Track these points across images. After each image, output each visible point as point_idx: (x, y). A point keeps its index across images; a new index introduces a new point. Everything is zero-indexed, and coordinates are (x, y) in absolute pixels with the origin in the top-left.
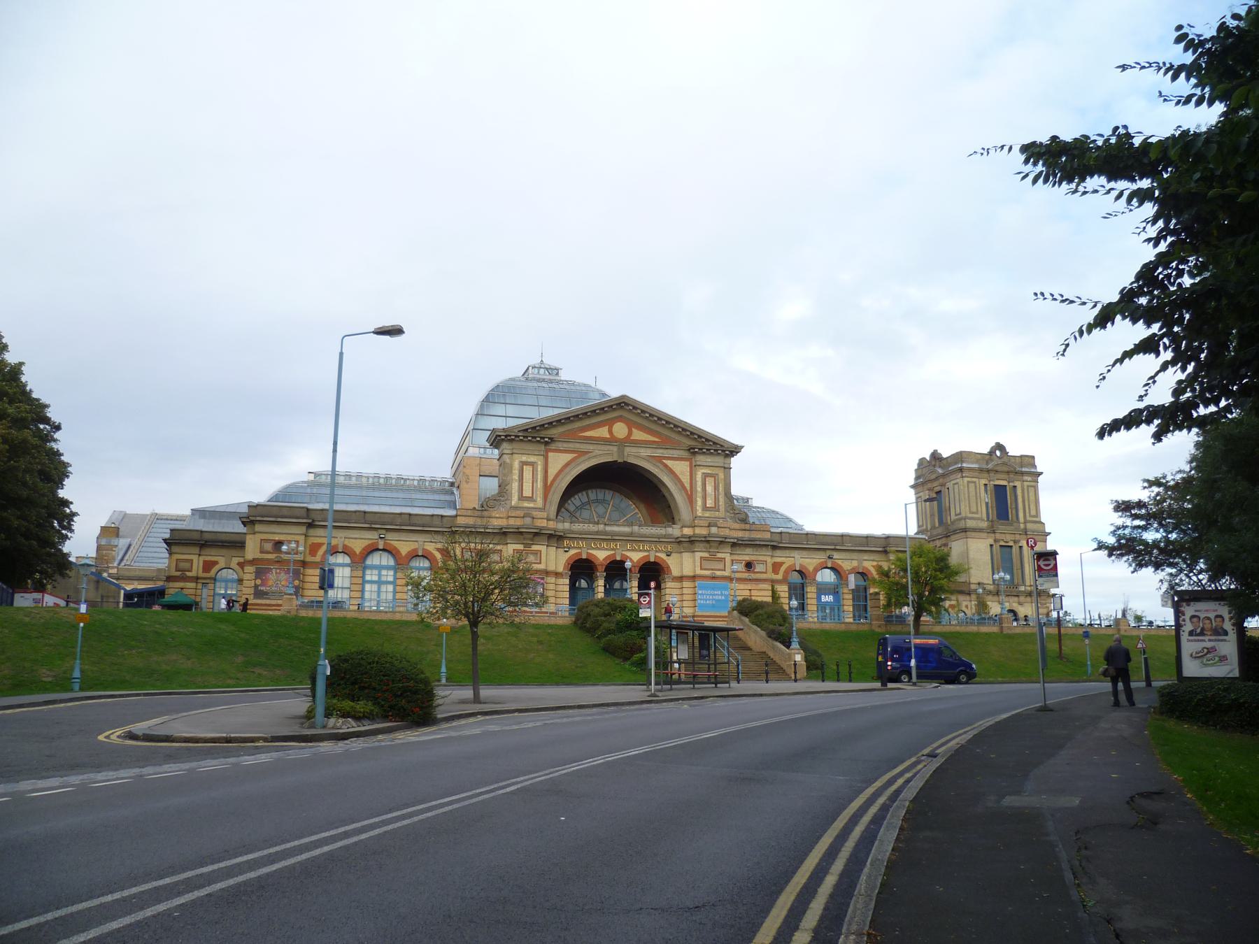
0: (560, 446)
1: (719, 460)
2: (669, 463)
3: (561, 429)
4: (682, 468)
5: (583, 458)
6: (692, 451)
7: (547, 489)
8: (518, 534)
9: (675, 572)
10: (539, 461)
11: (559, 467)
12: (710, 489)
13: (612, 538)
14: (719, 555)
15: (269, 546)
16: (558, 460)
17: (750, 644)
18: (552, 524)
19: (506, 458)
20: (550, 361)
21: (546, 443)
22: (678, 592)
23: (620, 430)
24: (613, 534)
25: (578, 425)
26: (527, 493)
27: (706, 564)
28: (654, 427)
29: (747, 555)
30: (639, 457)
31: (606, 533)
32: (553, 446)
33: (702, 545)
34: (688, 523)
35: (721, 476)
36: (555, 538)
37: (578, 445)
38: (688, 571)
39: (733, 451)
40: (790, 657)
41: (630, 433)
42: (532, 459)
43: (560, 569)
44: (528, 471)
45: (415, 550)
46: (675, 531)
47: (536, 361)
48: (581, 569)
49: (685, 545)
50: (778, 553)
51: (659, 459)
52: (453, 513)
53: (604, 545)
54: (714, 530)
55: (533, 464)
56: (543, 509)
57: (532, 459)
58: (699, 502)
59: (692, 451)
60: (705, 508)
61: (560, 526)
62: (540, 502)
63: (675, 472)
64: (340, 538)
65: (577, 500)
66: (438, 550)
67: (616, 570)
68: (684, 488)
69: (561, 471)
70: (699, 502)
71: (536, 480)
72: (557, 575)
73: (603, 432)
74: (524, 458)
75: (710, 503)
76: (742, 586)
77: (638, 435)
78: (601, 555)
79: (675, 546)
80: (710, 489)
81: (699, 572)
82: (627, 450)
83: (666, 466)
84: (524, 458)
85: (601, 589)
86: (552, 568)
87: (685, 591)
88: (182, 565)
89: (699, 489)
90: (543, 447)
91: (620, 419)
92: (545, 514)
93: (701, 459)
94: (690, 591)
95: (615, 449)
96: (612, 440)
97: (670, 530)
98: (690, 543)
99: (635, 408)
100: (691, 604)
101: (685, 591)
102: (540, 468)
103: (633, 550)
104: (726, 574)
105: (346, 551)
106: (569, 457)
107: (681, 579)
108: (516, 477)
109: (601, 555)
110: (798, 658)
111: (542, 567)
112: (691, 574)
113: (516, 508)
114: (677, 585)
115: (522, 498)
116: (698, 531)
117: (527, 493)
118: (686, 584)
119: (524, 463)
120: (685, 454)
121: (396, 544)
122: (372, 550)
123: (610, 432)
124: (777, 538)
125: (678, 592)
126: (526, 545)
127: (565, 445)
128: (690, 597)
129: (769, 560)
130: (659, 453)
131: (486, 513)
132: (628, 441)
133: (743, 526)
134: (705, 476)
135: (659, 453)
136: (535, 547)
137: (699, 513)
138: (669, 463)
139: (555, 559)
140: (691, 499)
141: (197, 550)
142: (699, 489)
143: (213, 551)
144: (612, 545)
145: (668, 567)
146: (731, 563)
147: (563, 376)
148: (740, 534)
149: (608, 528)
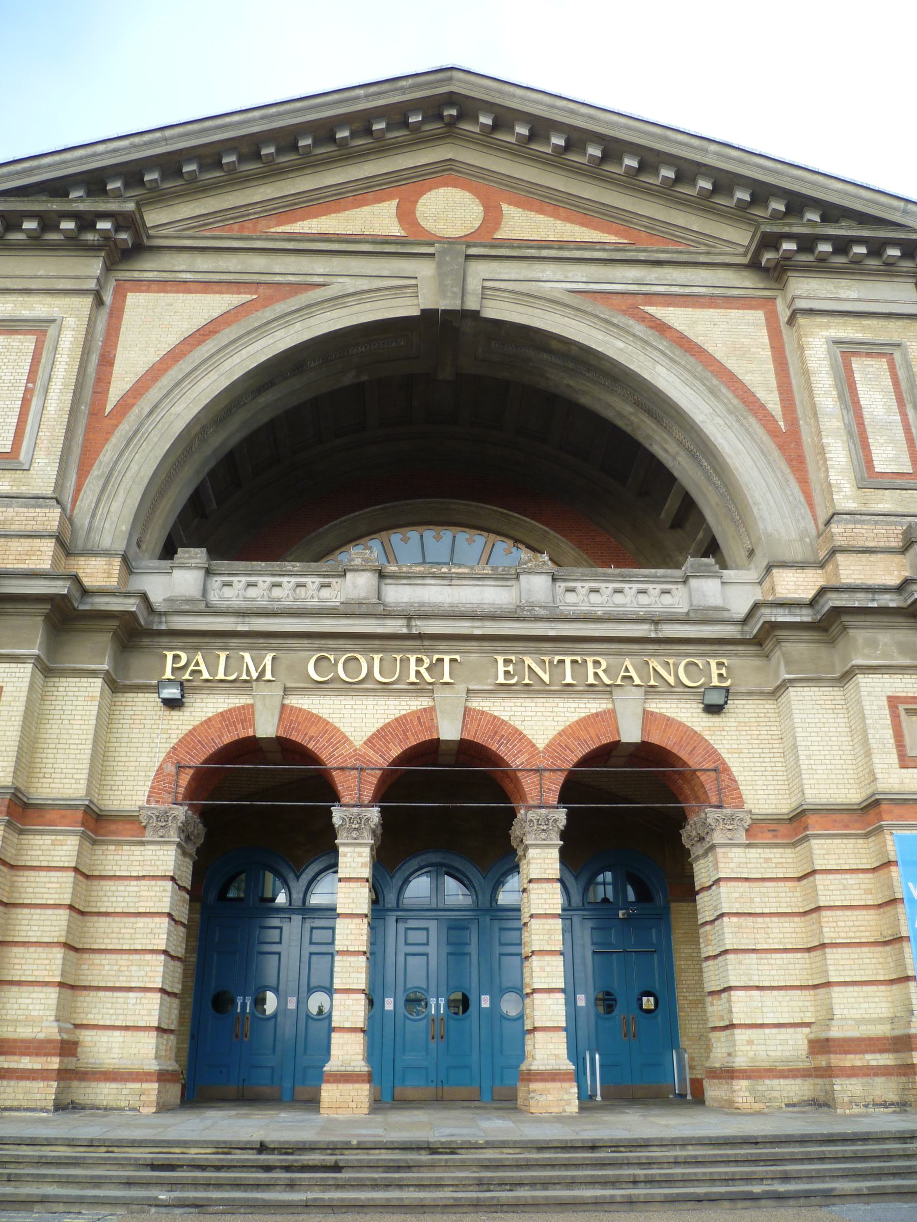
0: (180, 263)
2: (676, 317)
5: (280, 308)
6: (769, 265)
7: (92, 420)
9: (761, 790)
10: (71, 317)
11: (172, 340)
22: (789, 898)
23: (449, 210)
32: (149, 267)
33: (885, 638)
34: (797, 552)
37: (259, 263)
38: (832, 781)
41: (492, 217)
46: (727, 593)
49: (798, 648)
53: (372, 664)
57: (39, 308)
58: (838, 454)
60: (869, 478)
62: (42, 474)
67: (448, 805)
68: (751, 403)
69: (174, 356)
70: (838, 454)
72: (97, 823)
78: (357, 722)
79: (744, 668)
81: (894, 779)
82: (479, 272)
83: (661, 328)
86: (64, 778)
87: (829, 890)
89: (826, 397)
90: (95, 266)
92: (51, 518)
94: (858, 890)
95: (425, 270)
99: (504, 118)
100: (872, 963)
101: (829, 890)
102: (69, 342)
103: (532, 689)
107: (797, 825)
109: (357, 722)
112: (854, 796)
114: (779, 860)
118: (828, 851)
123: (406, 215)
125: (789, 898)
127: (204, 263)
128: (866, 925)
132: (484, 246)
134: (846, 352)
138: (676, 317)
140: (792, 447)
142: (826, 397)
144: (415, 666)
145: (721, 769)
149: (398, 594)
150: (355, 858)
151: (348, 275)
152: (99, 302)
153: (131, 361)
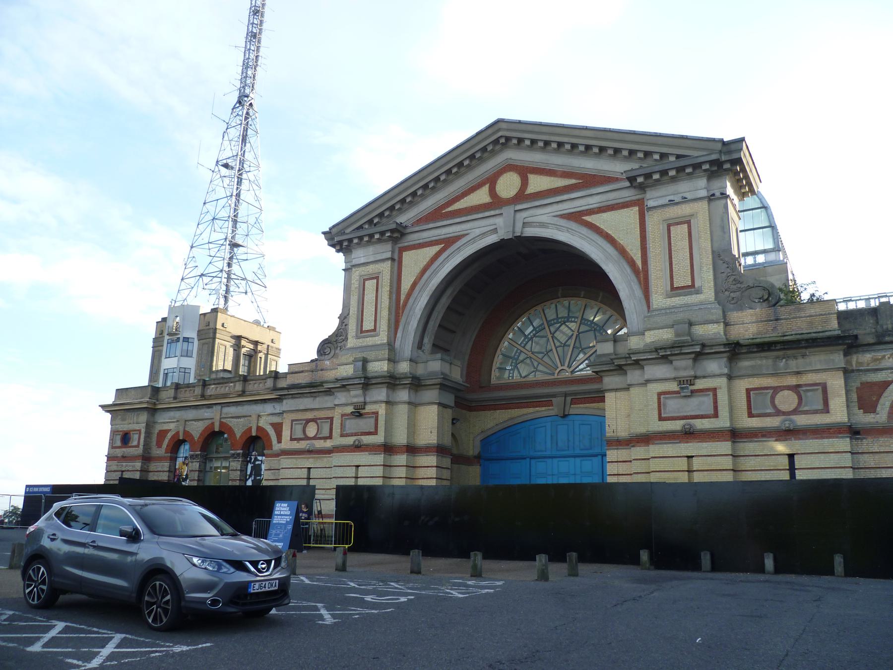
1: (699, 186)
4: (622, 224)
7: (398, 310)
10: (385, 269)
11: (418, 270)
14: (700, 384)
16: (414, 261)
21: (394, 240)
27: (673, 406)
39: (724, 162)
51: (576, 217)
66: (273, 425)
72: (412, 450)
73: (482, 196)
91: (510, 167)
93: (654, 197)
104: (723, 422)
111: (379, 439)
120: (629, 194)
137: (659, 300)
140: (642, 276)
152: (393, 259)
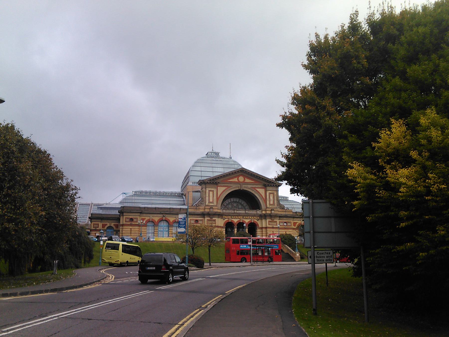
1: (275, 188)
2: (257, 189)
3: (222, 179)
4: (262, 191)
7: (218, 199)
8: (209, 215)
9: (260, 226)
10: (215, 190)
12: (271, 198)
13: (239, 215)
14: (275, 220)
15: (128, 220)
16: (221, 189)
17: (284, 250)
18: (219, 211)
19: (204, 189)
20: (216, 150)
23: (241, 179)
24: (239, 213)
25: (227, 177)
26: (211, 200)
28: (252, 177)
29: (285, 220)
30: (248, 188)
31: (238, 213)
32: (219, 185)
35: (275, 193)
36: (220, 215)
38: (264, 226)
40: (296, 254)
41: (245, 180)
42: (212, 189)
43: (222, 225)
44: (211, 193)
45: (175, 220)
46: (259, 212)
47: (211, 151)
48: (229, 225)
50: (295, 219)
51: (255, 188)
52: (187, 207)
54: (273, 212)
55: (213, 191)
56: (216, 206)
57: (212, 189)
59: (265, 186)
60: (270, 204)
61: (221, 211)
62: (215, 204)
63: (260, 192)
64: (152, 217)
65: (227, 202)
71: (214, 197)
74: (210, 189)
75: (272, 203)
76: (283, 231)
77: (247, 180)
78: (236, 221)
80: (271, 198)
81: (268, 226)
82: (243, 186)
84: (210, 189)
85: (236, 232)
86: (220, 225)
88: (95, 226)
90: (216, 185)
91: (241, 175)
93: (268, 188)
95: (239, 185)
96: (239, 183)
97: (258, 212)
98: (264, 217)
105: (153, 222)
106: (224, 188)
107: (262, 228)
108: (207, 195)
109: (236, 221)
110: (298, 255)
113: (208, 206)
115: (209, 202)
116: (268, 212)
117: (211, 200)
119: (210, 191)
121: (169, 218)
122: (161, 220)
123: (238, 179)
124: (295, 214)
126: (211, 218)
129: (292, 221)
130: (254, 186)
131: (198, 208)
132: (244, 183)
133: (283, 210)
135: (254, 186)
136: (214, 219)
137: (268, 206)
138: (257, 189)
139: (220, 222)
141: (100, 221)
143: (106, 221)
146: (278, 222)
147: (221, 155)
148: (282, 213)
150: (236, 230)
151: (234, 186)
153: (219, 194)
